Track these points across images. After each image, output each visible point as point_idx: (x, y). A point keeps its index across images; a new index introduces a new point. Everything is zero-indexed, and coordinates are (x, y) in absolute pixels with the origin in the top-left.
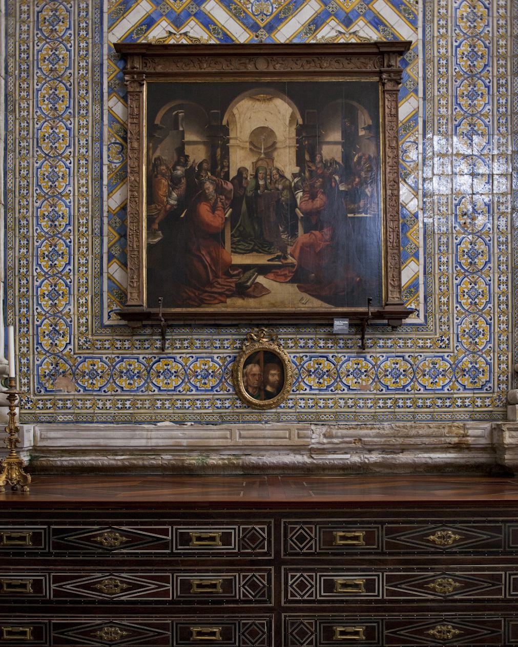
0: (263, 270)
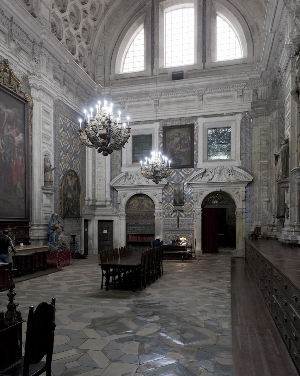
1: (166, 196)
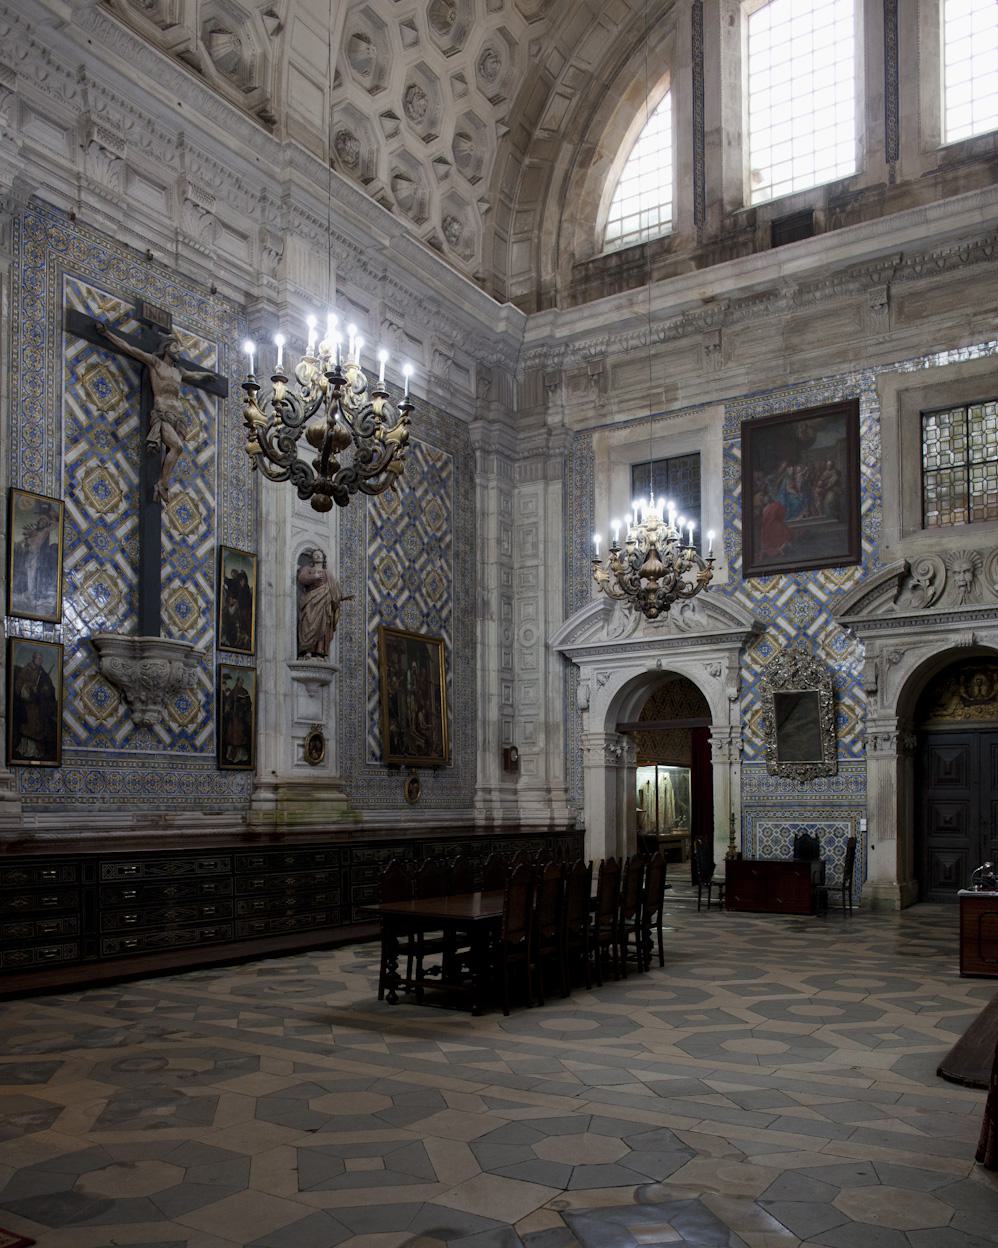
1: (756, 675)
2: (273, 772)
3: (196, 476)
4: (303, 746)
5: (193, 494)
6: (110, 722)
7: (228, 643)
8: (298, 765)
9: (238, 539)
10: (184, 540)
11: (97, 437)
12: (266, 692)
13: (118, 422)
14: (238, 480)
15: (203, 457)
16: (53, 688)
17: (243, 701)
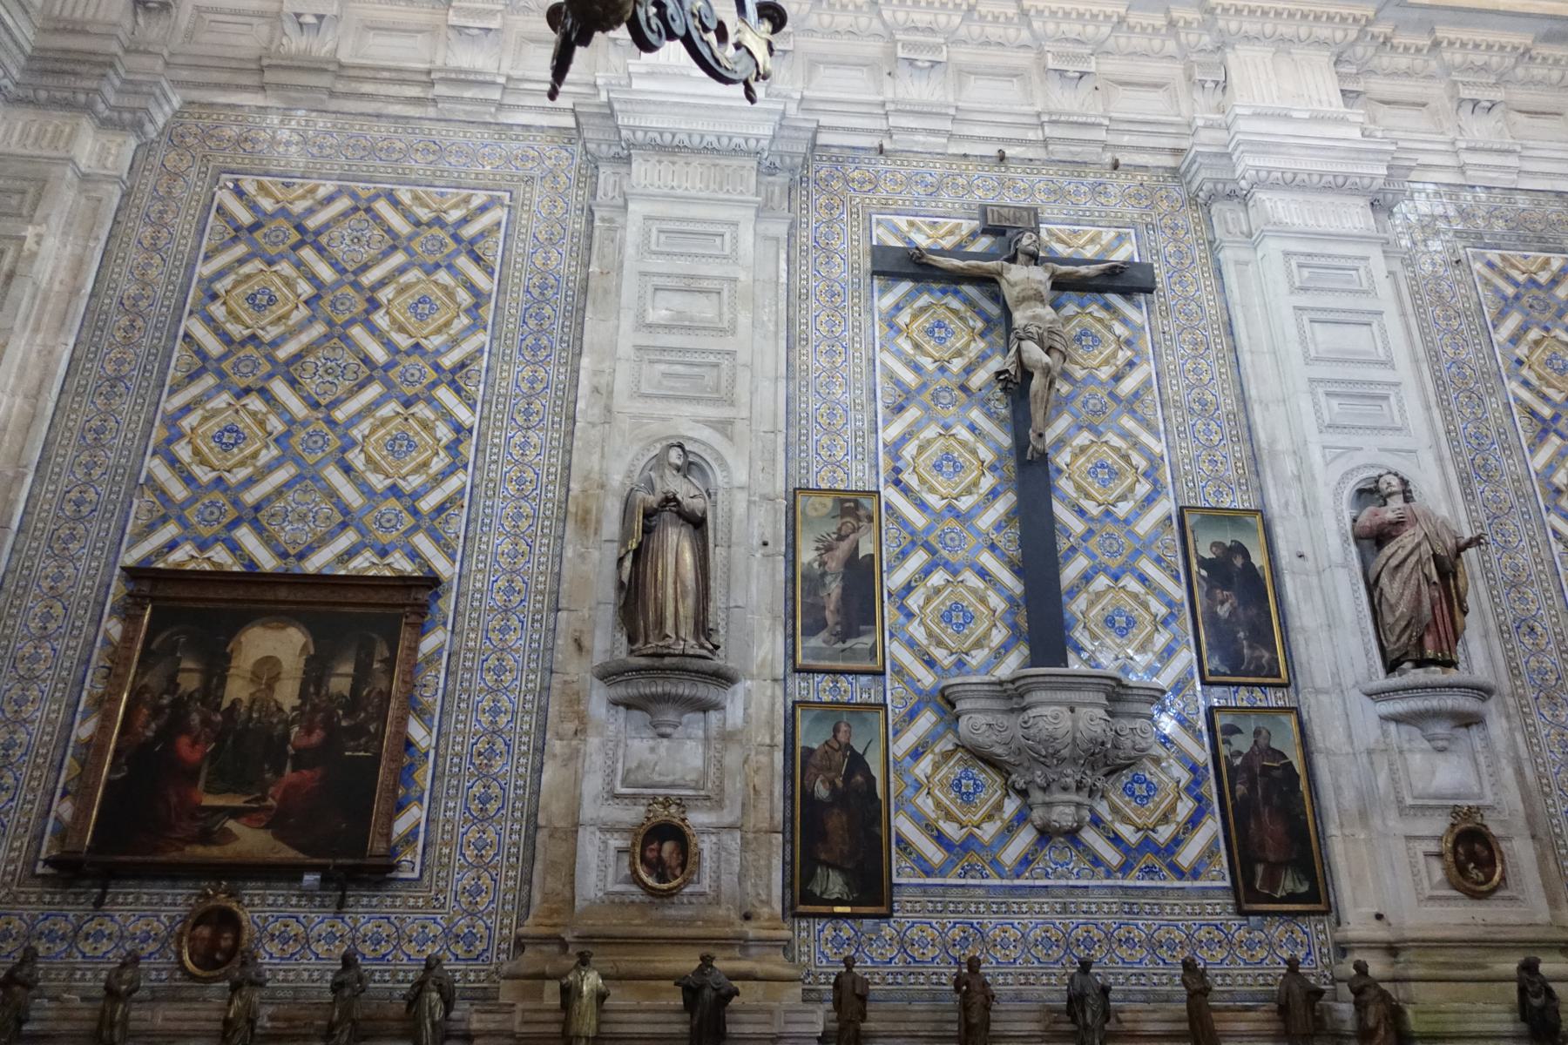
0: (235, 813)
2: (1379, 917)
3: (1120, 414)
4: (1440, 855)
5: (1116, 441)
6: (988, 831)
7: (1223, 669)
8: (1431, 898)
9: (1219, 493)
10: (1108, 513)
11: (935, 397)
12: (1328, 753)
13: (969, 370)
14: (1204, 404)
15: (1128, 386)
16: (871, 780)
17: (1276, 773)
